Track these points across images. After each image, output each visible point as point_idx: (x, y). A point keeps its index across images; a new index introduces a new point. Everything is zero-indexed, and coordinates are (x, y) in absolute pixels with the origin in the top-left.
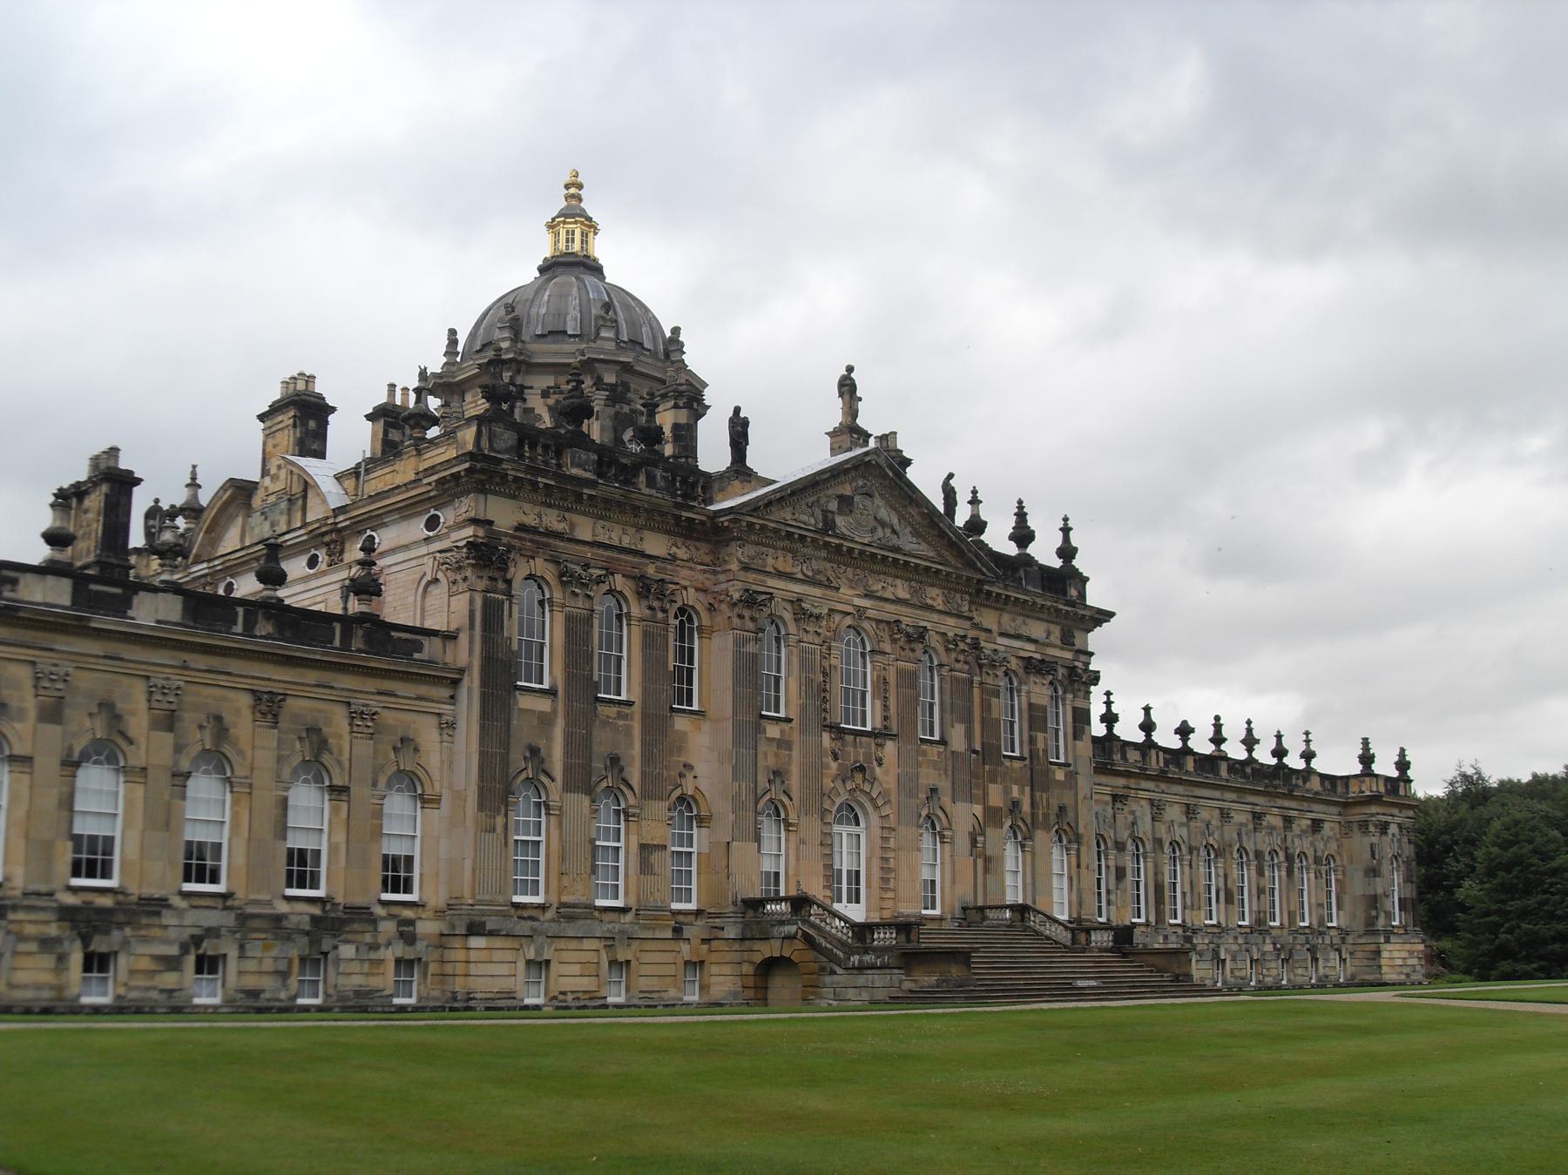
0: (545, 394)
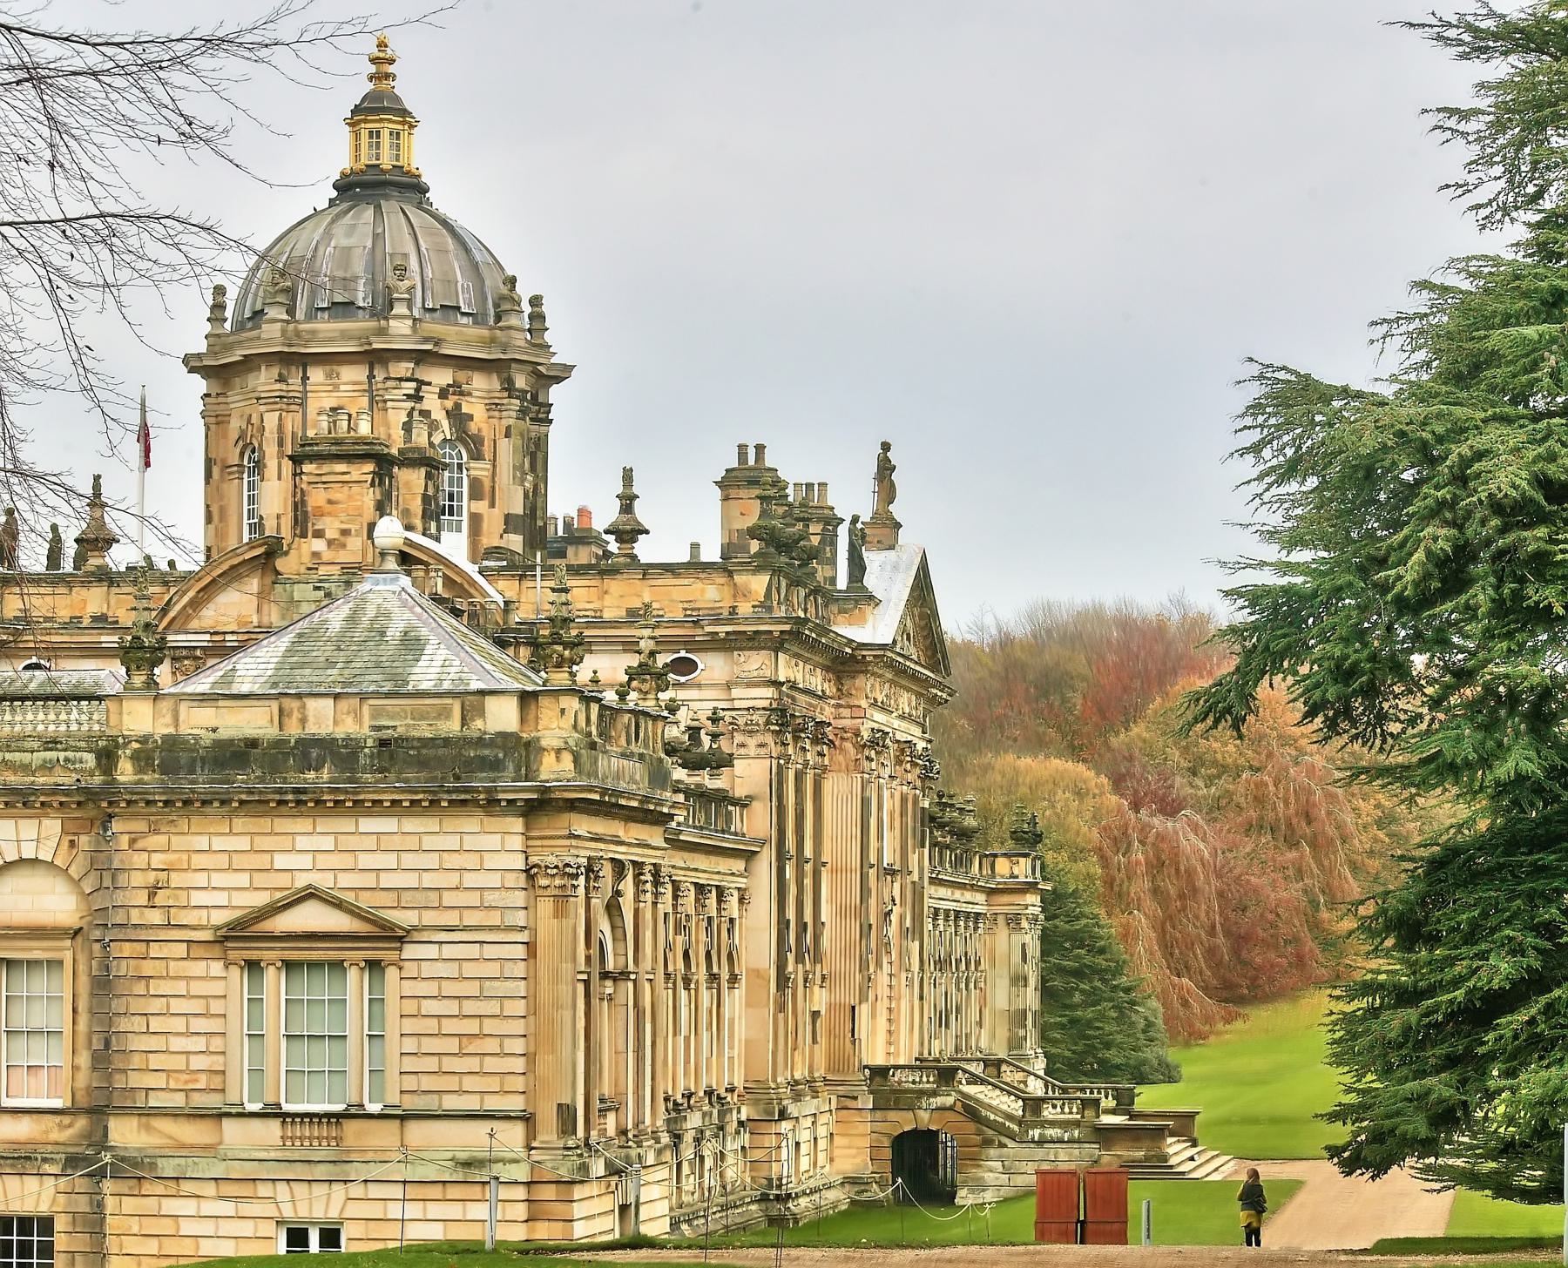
0: (443, 394)
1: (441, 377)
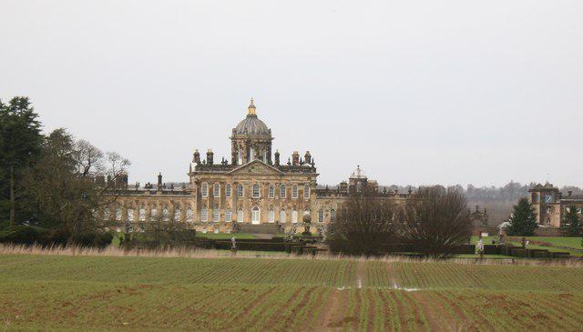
1: (238, 141)
